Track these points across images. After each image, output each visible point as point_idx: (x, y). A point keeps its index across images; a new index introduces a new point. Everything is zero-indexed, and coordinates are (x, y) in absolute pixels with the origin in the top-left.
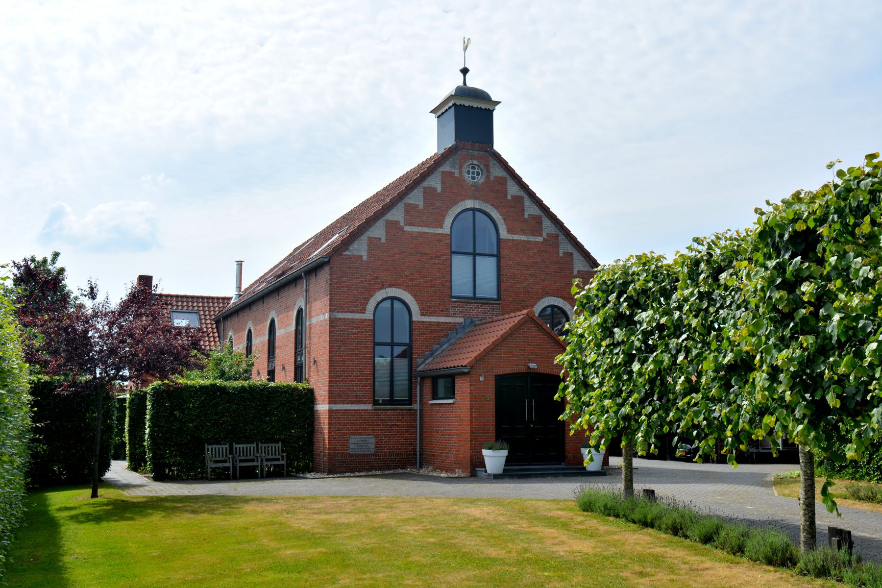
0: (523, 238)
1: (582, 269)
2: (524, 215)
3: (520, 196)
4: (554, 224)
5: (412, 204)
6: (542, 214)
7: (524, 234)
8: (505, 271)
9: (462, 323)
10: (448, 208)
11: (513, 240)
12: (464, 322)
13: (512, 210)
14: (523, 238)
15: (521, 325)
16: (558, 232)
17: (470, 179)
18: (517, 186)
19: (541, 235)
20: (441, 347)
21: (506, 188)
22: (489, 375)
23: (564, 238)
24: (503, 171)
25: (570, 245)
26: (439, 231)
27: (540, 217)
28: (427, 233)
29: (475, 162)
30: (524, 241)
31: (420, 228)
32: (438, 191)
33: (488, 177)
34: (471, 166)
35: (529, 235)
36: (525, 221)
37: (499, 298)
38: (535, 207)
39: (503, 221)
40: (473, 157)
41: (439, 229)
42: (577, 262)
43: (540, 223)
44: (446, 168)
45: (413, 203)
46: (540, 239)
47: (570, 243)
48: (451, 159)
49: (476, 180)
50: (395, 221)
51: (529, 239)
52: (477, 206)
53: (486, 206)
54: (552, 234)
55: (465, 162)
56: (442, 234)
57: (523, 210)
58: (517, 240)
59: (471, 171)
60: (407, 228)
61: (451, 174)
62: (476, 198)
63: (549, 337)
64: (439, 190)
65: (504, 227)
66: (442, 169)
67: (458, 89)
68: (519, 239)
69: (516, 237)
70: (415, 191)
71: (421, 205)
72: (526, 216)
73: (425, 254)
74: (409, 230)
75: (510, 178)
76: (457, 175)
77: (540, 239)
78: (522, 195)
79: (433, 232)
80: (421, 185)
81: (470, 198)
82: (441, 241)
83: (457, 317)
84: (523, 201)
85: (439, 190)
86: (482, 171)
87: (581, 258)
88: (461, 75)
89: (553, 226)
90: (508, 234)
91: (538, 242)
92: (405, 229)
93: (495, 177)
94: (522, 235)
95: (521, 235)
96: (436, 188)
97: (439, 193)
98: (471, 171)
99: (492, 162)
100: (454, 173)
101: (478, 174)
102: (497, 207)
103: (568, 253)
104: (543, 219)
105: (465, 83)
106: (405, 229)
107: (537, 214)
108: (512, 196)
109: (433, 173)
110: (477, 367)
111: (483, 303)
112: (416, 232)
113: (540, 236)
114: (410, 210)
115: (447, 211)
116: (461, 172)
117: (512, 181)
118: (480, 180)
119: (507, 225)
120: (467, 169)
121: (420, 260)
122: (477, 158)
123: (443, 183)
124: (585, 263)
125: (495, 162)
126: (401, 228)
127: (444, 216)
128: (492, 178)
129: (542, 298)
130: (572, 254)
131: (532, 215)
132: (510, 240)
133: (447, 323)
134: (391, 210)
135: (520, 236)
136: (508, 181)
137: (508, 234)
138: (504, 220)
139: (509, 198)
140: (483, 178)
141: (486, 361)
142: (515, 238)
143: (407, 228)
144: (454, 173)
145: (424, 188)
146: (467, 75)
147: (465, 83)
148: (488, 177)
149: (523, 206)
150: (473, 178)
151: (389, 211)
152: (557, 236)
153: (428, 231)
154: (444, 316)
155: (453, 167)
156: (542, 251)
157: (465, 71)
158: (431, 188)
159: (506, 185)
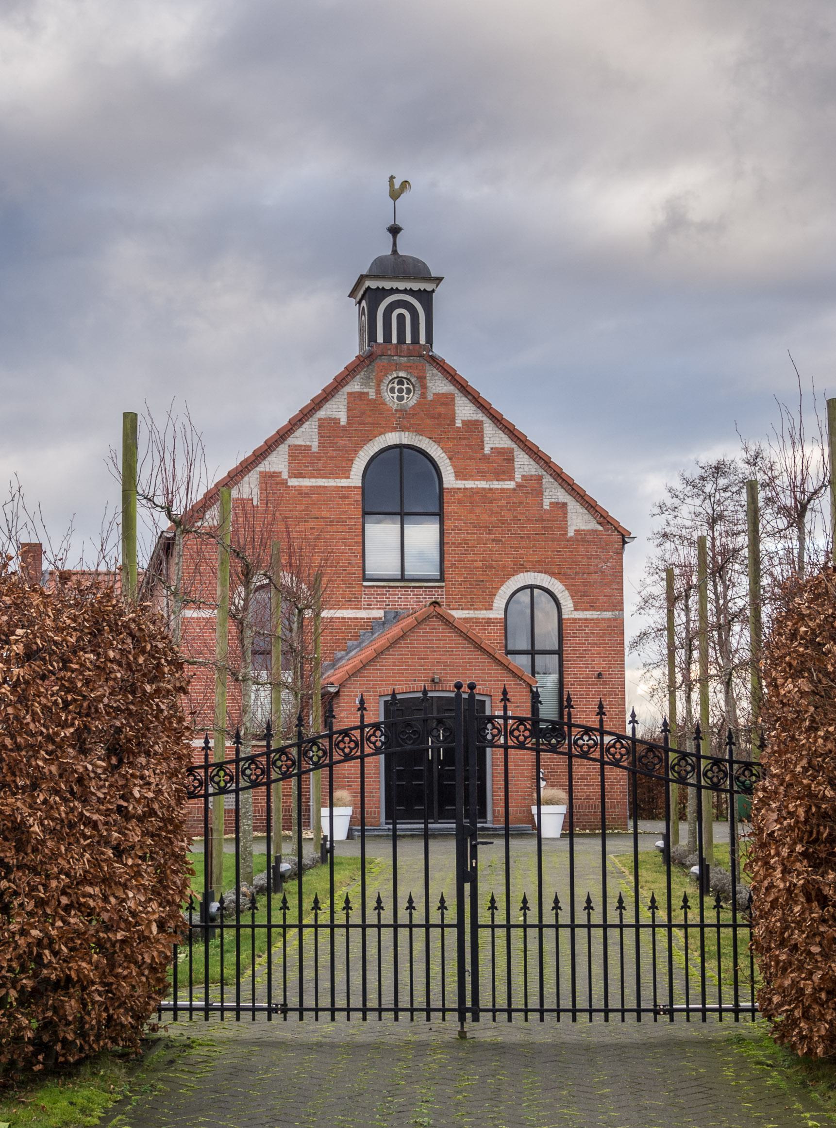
0: (483, 484)
1: (583, 528)
2: (483, 449)
3: (476, 421)
4: (534, 460)
5: (301, 446)
6: (514, 446)
7: (484, 478)
8: (449, 538)
9: (380, 618)
10: (358, 447)
11: (465, 489)
12: (385, 616)
13: (463, 442)
14: (483, 484)
15: (419, 623)
16: (541, 472)
17: (396, 400)
18: (471, 405)
19: (512, 479)
20: (347, 654)
21: (454, 410)
22: (371, 696)
23: (552, 480)
24: (448, 384)
25: (562, 490)
26: (344, 482)
27: (511, 450)
28: (325, 487)
29: (402, 374)
30: (484, 489)
31: (313, 480)
32: (342, 424)
33: (423, 395)
34: (396, 380)
35: (492, 480)
36: (486, 458)
37: (442, 579)
38: (503, 435)
39: (448, 461)
40: (398, 367)
41: (344, 480)
42: (574, 517)
43: (511, 460)
44: (355, 386)
45: (303, 443)
46: (511, 485)
47: (562, 487)
48: (362, 373)
49: (405, 401)
50: (274, 472)
51: (492, 486)
52: (405, 441)
53: (420, 441)
54: (531, 476)
55: (386, 375)
56: (349, 487)
57: (483, 442)
58: (472, 488)
59: (397, 387)
60: (293, 482)
61: (362, 395)
62: (403, 429)
63: (465, 639)
64: (343, 421)
65: (450, 469)
66: (348, 389)
67: (379, 262)
68: (474, 486)
69: (470, 484)
70: (306, 425)
71: (315, 446)
72: (487, 450)
73: (322, 518)
74: (296, 484)
75: (460, 394)
76: (372, 395)
77: (511, 485)
78: (481, 419)
79: (335, 484)
80: (315, 416)
81: (394, 429)
82: (348, 497)
83: (373, 609)
84: (482, 429)
85: (343, 421)
86: (414, 386)
87: (582, 511)
88: (390, 236)
89: (533, 463)
90: (456, 479)
91: (507, 489)
92: (289, 484)
93: (434, 394)
94: (480, 480)
95: (477, 480)
96: (339, 419)
97: (343, 426)
98: (397, 387)
99: (431, 372)
100: (368, 393)
101: (409, 391)
102: (438, 441)
103: (558, 503)
104: (515, 453)
105: (395, 252)
106: (289, 484)
107: (506, 446)
108: (463, 421)
109: (333, 396)
110: (352, 684)
111: (415, 587)
112: (307, 487)
113: (510, 480)
114: (298, 454)
115: (356, 452)
116: (378, 392)
117: (464, 398)
118: (411, 401)
119: (454, 467)
120: (390, 386)
121: (314, 528)
122: (406, 369)
123: (349, 410)
124: (588, 517)
125: (435, 371)
126: (284, 483)
127: (352, 461)
128: (430, 397)
129: (513, 575)
130: (565, 505)
131: (497, 448)
132: (459, 489)
133: (357, 618)
134: (267, 456)
135: (477, 482)
136: (457, 398)
137: (456, 479)
138: (450, 459)
139: (459, 424)
140: (415, 398)
141: (365, 677)
142: (468, 486)
143: (293, 482)
144: (368, 393)
145: (319, 419)
146: (399, 236)
147: (395, 252)
148: (423, 395)
149: (483, 435)
150: (400, 399)
151: (265, 458)
152: (540, 479)
153: (326, 484)
154: (352, 609)
155: (365, 383)
156: (514, 503)
157: (395, 230)
158: (330, 419)
159: (454, 405)
